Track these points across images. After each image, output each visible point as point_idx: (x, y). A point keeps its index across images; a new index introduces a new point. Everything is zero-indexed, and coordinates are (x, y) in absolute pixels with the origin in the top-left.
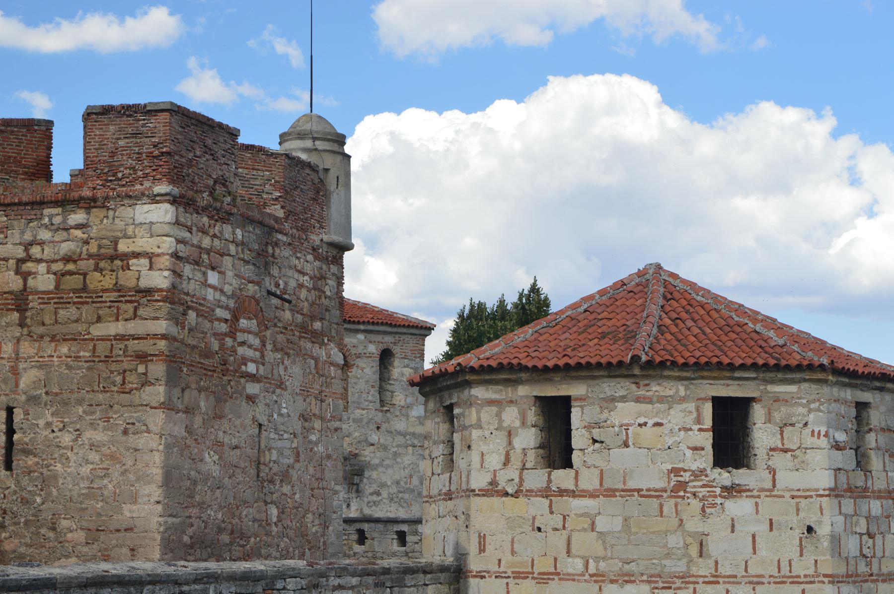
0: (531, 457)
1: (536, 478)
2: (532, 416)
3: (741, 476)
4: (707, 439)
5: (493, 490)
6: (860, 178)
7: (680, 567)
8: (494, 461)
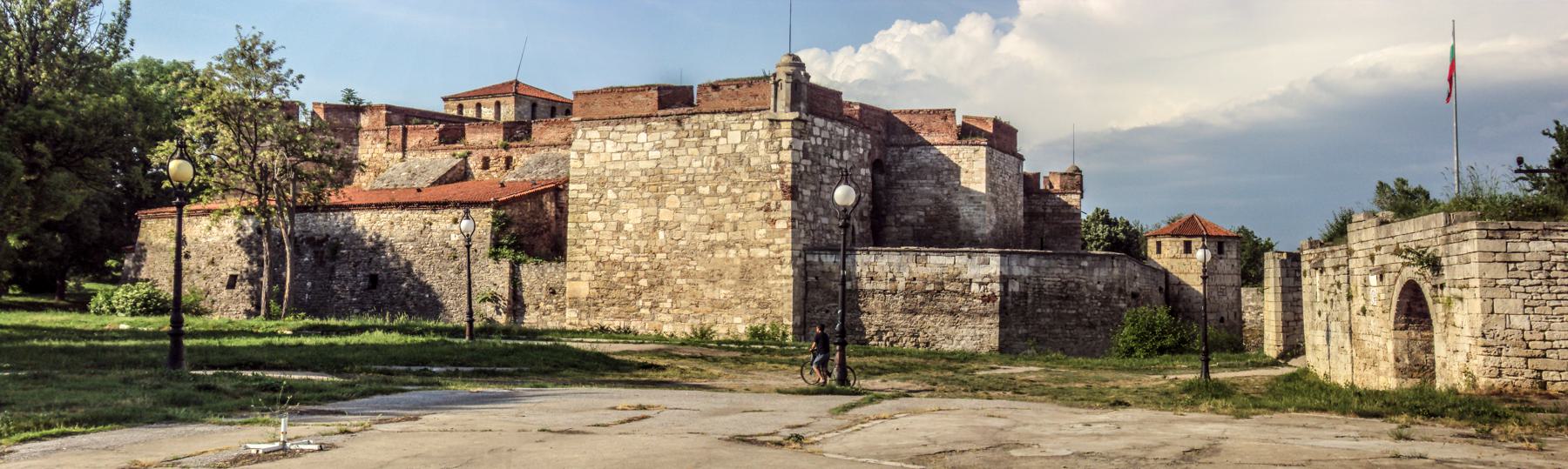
1: (1184, 256)
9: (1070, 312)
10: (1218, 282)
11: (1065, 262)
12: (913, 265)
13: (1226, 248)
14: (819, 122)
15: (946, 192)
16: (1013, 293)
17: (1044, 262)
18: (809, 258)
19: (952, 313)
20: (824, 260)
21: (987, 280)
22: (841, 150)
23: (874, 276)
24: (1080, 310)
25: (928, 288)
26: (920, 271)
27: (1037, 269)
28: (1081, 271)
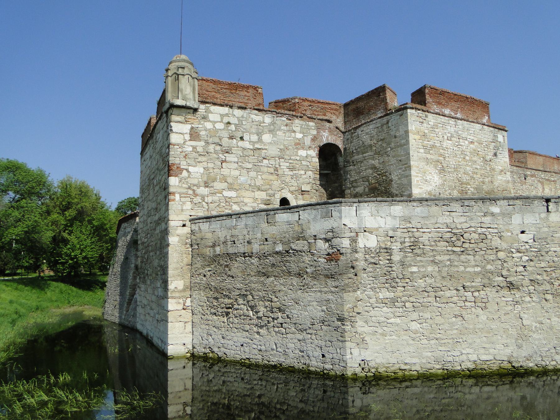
11: (460, 209)
12: (264, 225)
14: (213, 108)
15: (382, 160)
16: (368, 251)
18: (194, 227)
19: (299, 275)
20: (202, 228)
22: (259, 134)
24: (489, 267)
25: (277, 250)
26: (271, 231)
27: (407, 219)
28: (487, 220)
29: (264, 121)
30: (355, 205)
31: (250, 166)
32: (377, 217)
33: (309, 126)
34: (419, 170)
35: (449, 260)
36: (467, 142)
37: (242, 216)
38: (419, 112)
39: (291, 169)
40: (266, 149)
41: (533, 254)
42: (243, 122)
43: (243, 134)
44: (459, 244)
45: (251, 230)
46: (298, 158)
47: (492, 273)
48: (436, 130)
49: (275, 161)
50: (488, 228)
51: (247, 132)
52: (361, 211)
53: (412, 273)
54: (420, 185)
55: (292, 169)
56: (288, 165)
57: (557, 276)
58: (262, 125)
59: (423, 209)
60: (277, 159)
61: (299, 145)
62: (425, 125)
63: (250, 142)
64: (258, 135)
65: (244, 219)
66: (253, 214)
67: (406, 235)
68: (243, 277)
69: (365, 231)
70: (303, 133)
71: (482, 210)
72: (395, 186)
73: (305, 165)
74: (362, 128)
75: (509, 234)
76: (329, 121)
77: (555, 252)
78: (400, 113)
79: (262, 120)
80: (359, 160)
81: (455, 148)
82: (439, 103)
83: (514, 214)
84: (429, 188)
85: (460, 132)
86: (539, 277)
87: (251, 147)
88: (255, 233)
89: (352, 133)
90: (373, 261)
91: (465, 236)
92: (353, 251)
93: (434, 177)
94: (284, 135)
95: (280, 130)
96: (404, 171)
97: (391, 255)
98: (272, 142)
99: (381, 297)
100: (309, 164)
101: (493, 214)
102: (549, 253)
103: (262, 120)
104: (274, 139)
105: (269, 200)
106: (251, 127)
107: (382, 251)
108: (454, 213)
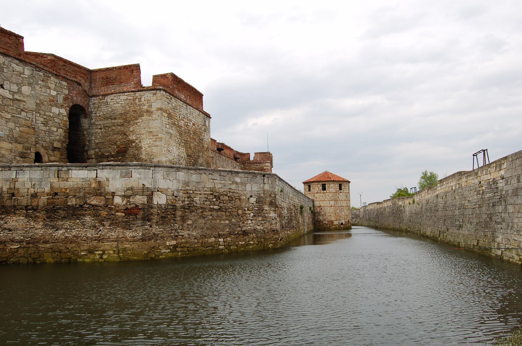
0: (321, 190)
1: (322, 192)
2: (321, 186)
3: (341, 191)
4: (339, 188)
5: (317, 193)
6: (422, 178)
7: (336, 199)
8: (317, 190)
9: (222, 222)
10: (339, 205)
13: (343, 187)
16: (159, 206)
17: (194, 176)
21: (130, 193)
23: (16, 192)
27: (187, 184)
29: (24, 72)
30: (152, 169)
31: (9, 116)
32: (167, 180)
33: (62, 85)
34: (166, 142)
35: (211, 215)
36: (191, 124)
37: (24, 169)
38: (167, 94)
39: (46, 125)
40: (24, 102)
41: (256, 211)
42: (5, 69)
43: (4, 82)
44: (217, 203)
45: (37, 183)
46: (52, 115)
47: (235, 225)
48: (176, 111)
49: (33, 115)
50: (234, 192)
51: (7, 81)
52: (156, 174)
53: (188, 225)
54: (166, 154)
55: (45, 124)
56: (42, 120)
57: (267, 226)
58: (22, 76)
59: (197, 176)
60: (34, 113)
61: (53, 102)
62: (170, 105)
63: (10, 91)
64: (17, 86)
65: (28, 172)
66: (40, 169)
67: (186, 195)
68: (25, 229)
69: (158, 191)
70: (57, 91)
71: (230, 180)
72: (144, 153)
73: (56, 123)
74: (112, 97)
75: (245, 197)
76: (79, 84)
77: (266, 210)
78: (153, 92)
79: (22, 71)
80: (107, 125)
81: (185, 127)
82: (179, 90)
83: (247, 184)
84: (171, 158)
85: (188, 115)
86: (258, 227)
87: (11, 97)
88: (42, 187)
89: (101, 99)
90: (163, 215)
91: (221, 197)
92: (149, 206)
93: (173, 149)
94: (40, 89)
95: (37, 84)
96: (154, 141)
97: (175, 211)
98: (31, 95)
99: (168, 244)
100: (60, 122)
101: (236, 183)
102: (264, 211)
103: (22, 71)
104: (33, 92)
105: (25, 153)
106: (12, 76)
107: (169, 207)
108: (215, 180)
